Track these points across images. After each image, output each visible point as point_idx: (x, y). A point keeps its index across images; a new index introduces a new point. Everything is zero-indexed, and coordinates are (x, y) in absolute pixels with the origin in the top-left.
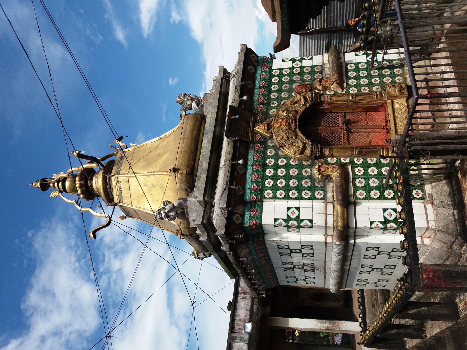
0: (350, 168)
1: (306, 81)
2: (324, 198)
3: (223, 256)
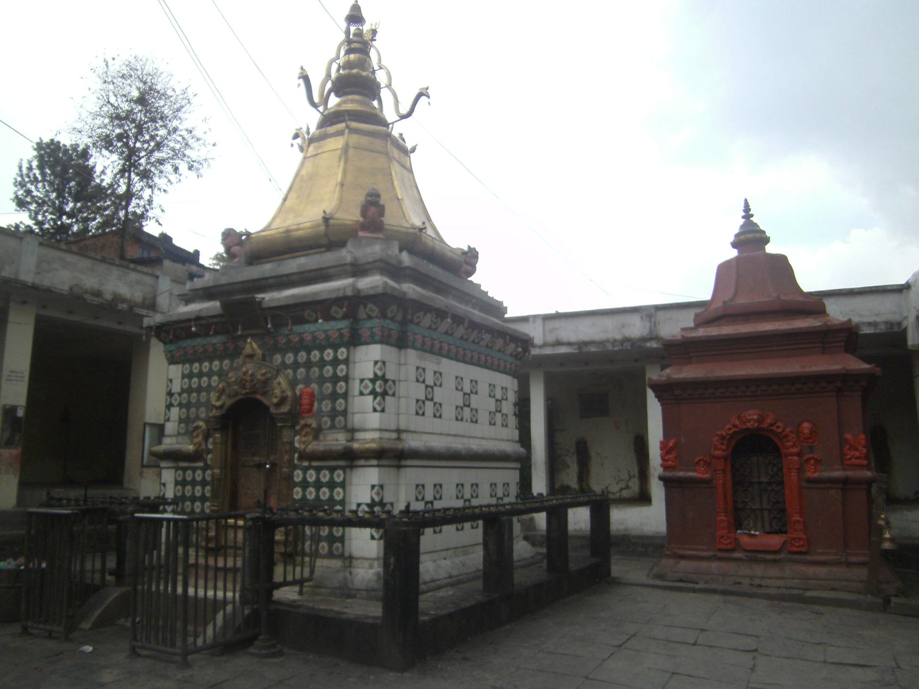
0: (201, 464)
1: (320, 403)
2: (179, 434)
3: (307, 313)
